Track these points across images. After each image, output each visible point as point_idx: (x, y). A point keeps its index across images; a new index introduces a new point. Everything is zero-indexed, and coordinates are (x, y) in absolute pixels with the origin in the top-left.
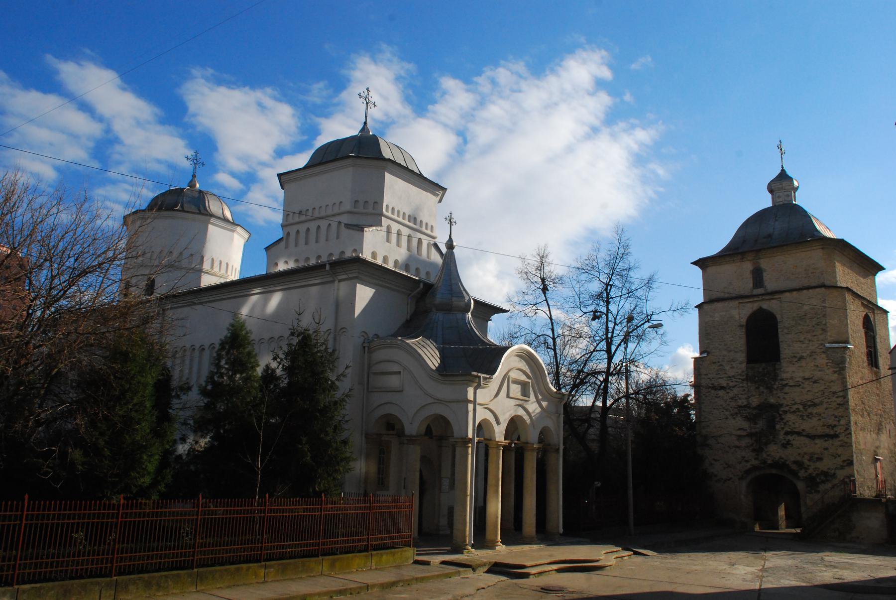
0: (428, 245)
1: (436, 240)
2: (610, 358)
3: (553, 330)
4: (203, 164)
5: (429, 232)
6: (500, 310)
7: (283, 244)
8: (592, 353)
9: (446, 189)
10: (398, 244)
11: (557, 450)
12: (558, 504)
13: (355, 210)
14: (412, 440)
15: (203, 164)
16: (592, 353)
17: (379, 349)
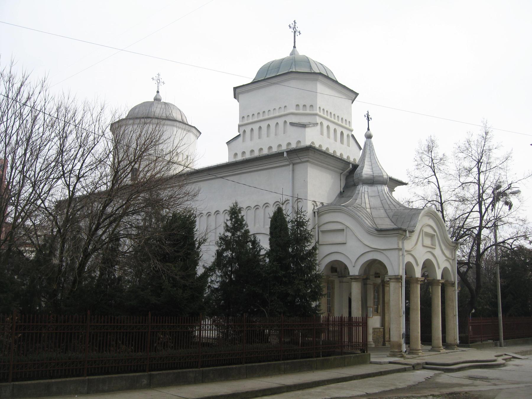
0: (348, 136)
1: (353, 133)
2: (482, 217)
3: (441, 197)
4: (164, 83)
5: (347, 126)
6: (401, 183)
7: (241, 139)
8: (470, 213)
9: (357, 94)
10: (329, 137)
11: (453, 284)
14: (355, 278)
15: (164, 83)
16: (470, 213)
17: (326, 213)
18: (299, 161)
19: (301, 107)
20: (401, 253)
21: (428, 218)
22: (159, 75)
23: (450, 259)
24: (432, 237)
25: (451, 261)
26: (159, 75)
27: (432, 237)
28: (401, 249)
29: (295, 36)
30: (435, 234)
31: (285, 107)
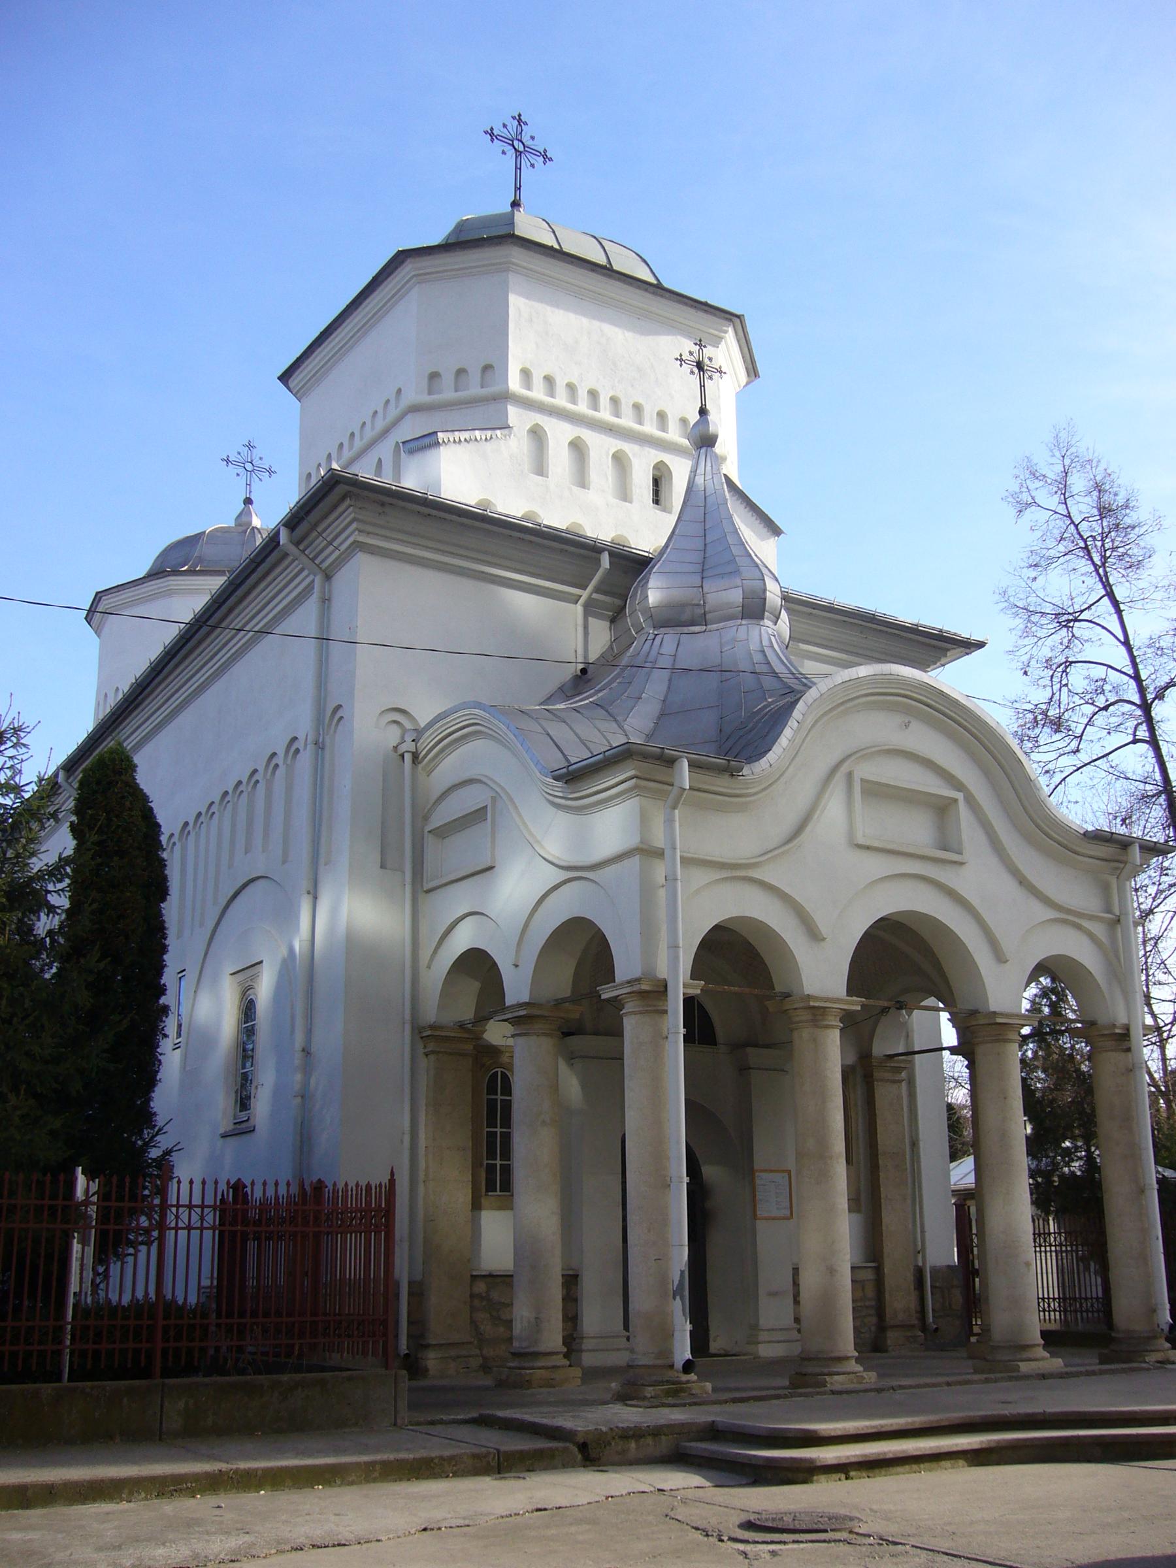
12: (1145, 1232)
13: (436, 398)
15: (270, 472)
18: (337, 553)
19: (448, 379)
20: (660, 871)
21: (898, 719)
22: (250, 446)
23: (1091, 918)
24: (942, 809)
25: (1099, 930)
26: (250, 446)
27: (942, 809)
28: (659, 854)
29: (518, 168)
30: (959, 796)
31: (399, 391)
